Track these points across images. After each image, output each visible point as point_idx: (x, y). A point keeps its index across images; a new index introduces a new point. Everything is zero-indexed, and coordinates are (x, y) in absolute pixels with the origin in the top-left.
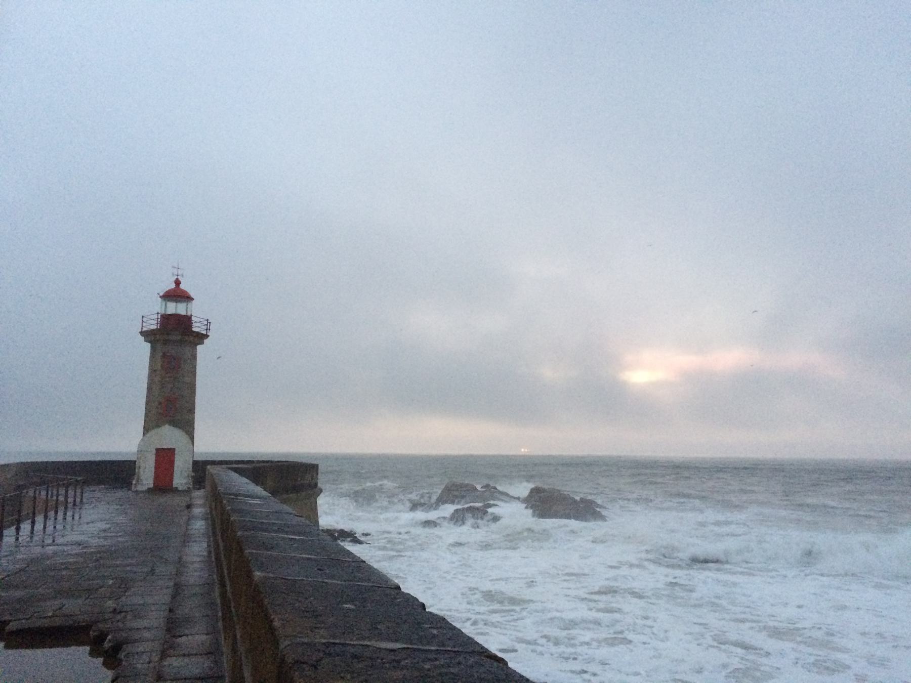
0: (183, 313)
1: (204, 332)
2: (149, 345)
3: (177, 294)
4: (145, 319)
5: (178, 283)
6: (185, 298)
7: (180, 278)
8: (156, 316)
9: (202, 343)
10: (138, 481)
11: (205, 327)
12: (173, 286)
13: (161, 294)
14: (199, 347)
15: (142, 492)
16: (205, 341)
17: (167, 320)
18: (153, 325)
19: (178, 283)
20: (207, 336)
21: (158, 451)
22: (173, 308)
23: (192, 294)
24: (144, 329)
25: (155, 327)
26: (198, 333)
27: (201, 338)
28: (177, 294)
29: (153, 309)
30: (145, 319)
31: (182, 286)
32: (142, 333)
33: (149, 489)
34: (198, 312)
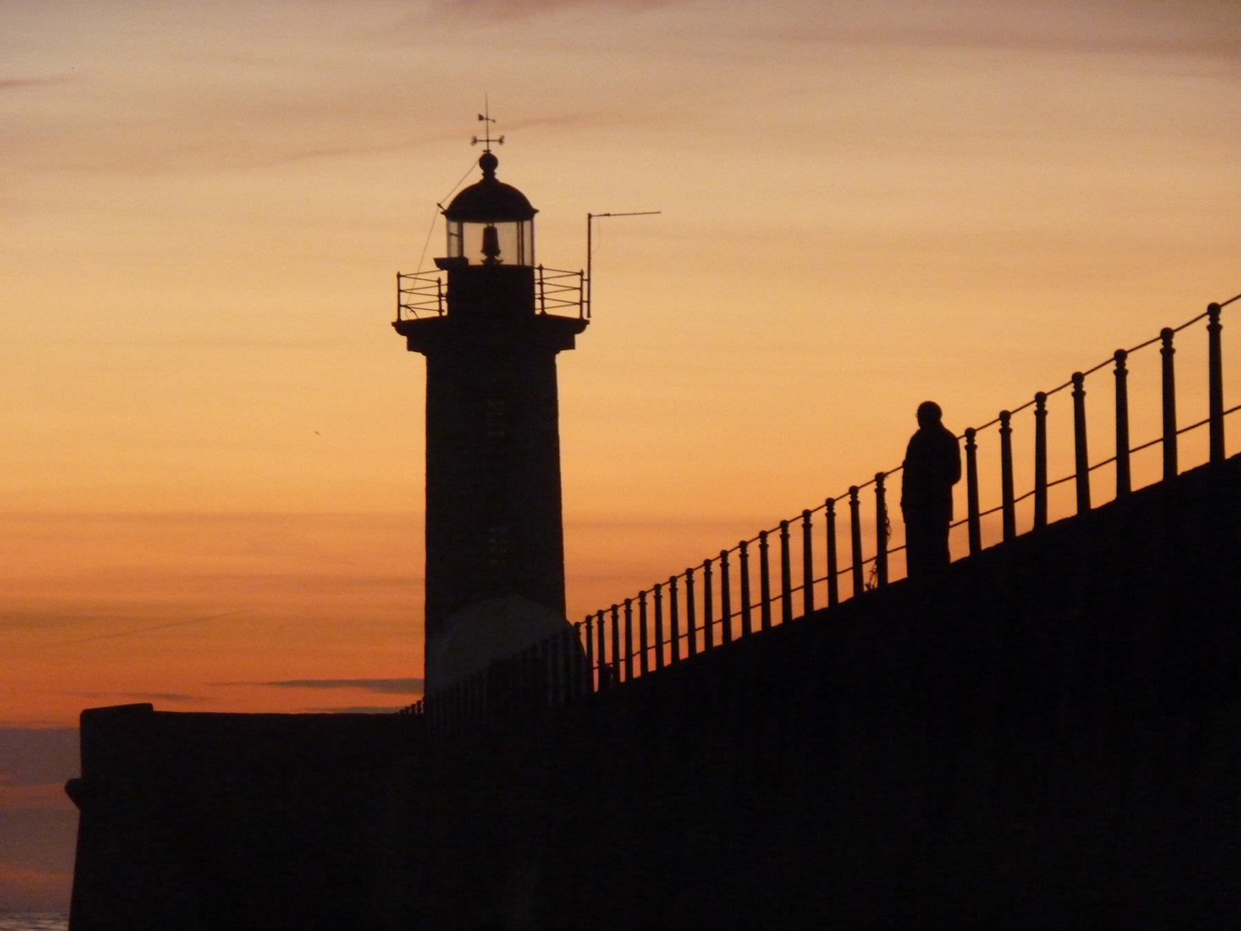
1: (573, 312)
2: (419, 362)
4: (405, 284)
5: (488, 162)
6: (516, 208)
7: (495, 150)
9: (570, 345)
12: (477, 176)
13: (446, 206)
14: (563, 359)
16: (578, 338)
18: (428, 304)
19: (488, 162)
20: (580, 325)
23: (534, 205)
24: (406, 316)
27: (565, 332)
30: (405, 284)
31: (502, 175)
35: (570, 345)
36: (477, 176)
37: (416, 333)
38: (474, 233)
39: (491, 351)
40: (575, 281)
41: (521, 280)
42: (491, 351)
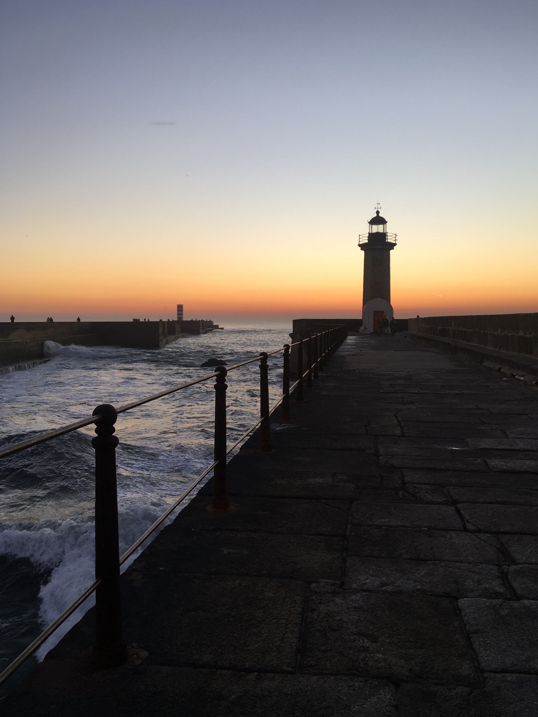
0: (381, 231)
1: (394, 242)
2: (363, 252)
3: (378, 220)
5: (378, 212)
8: (368, 235)
9: (393, 249)
10: (365, 328)
11: (394, 239)
14: (391, 251)
15: (368, 334)
17: (371, 236)
19: (378, 212)
20: (395, 244)
21: (375, 312)
22: (376, 229)
24: (360, 243)
25: (367, 241)
26: (389, 242)
27: (392, 246)
28: (378, 220)
29: (363, 231)
31: (380, 215)
32: (359, 245)
33: (371, 333)
34: (392, 230)
35: (393, 249)
36: (375, 215)
37: (362, 246)
39: (377, 250)
40: (395, 236)
42: (377, 250)
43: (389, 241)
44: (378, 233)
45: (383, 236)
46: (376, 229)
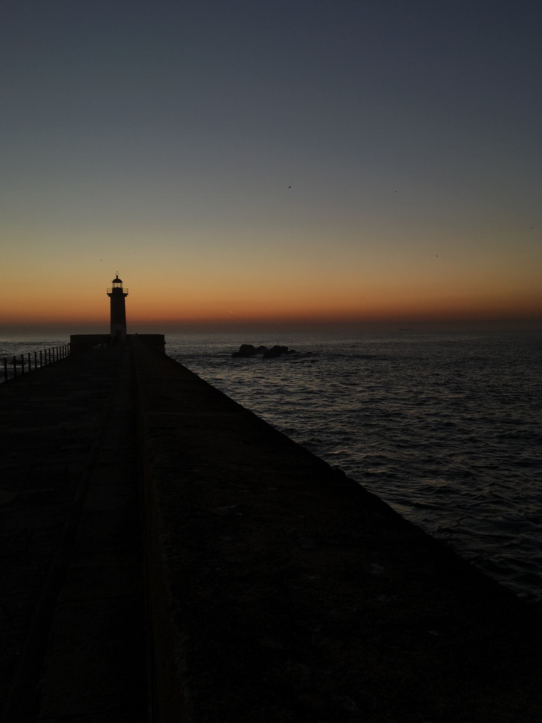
3: (117, 281)
5: (117, 276)
17: (114, 289)
19: (117, 276)
22: (117, 285)
27: (126, 295)
28: (117, 281)
29: (110, 286)
32: (108, 294)
34: (125, 286)
38: (116, 284)
39: (118, 296)
41: (121, 289)
42: (118, 296)
43: (124, 292)
44: (117, 288)
45: (121, 289)
46: (117, 285)
